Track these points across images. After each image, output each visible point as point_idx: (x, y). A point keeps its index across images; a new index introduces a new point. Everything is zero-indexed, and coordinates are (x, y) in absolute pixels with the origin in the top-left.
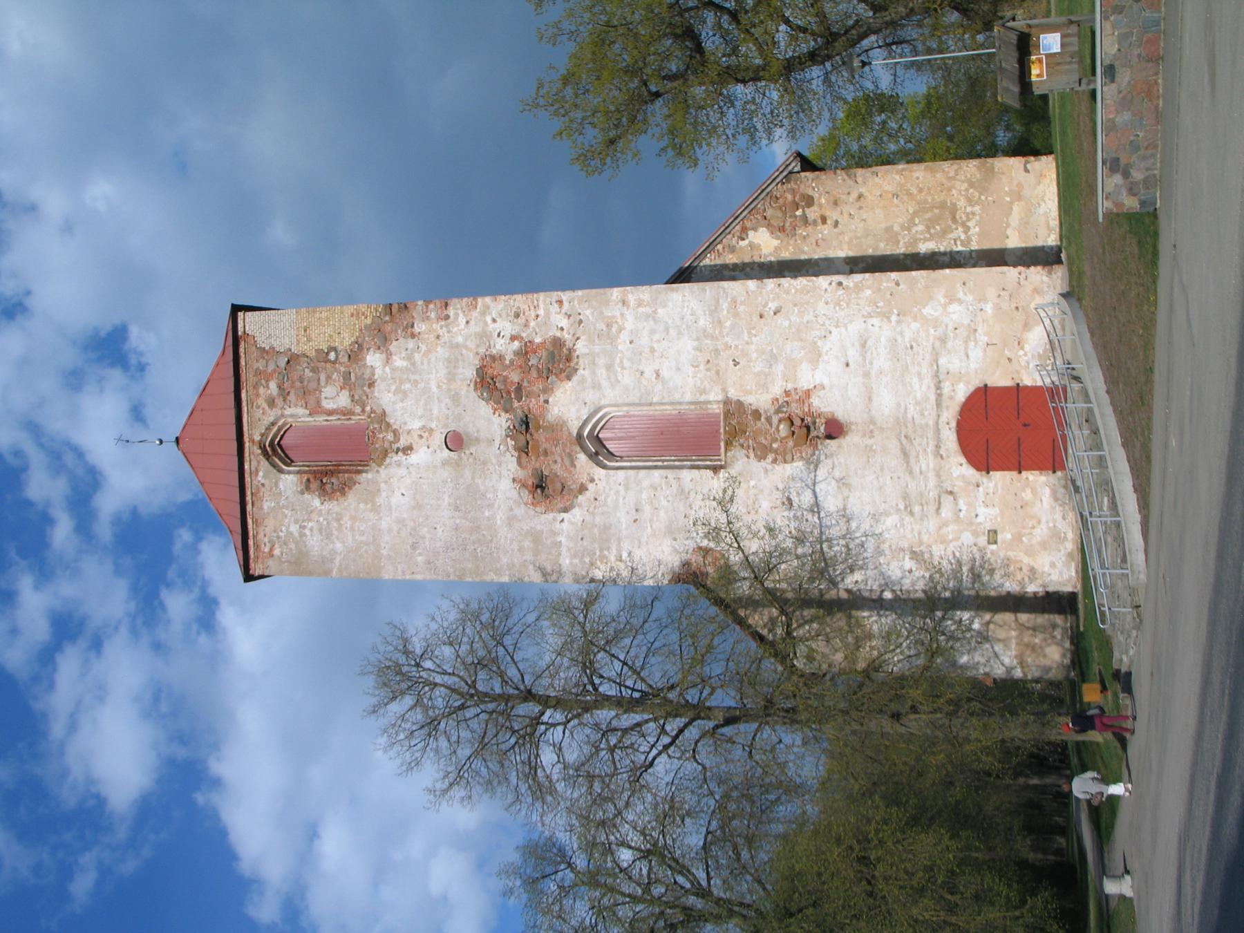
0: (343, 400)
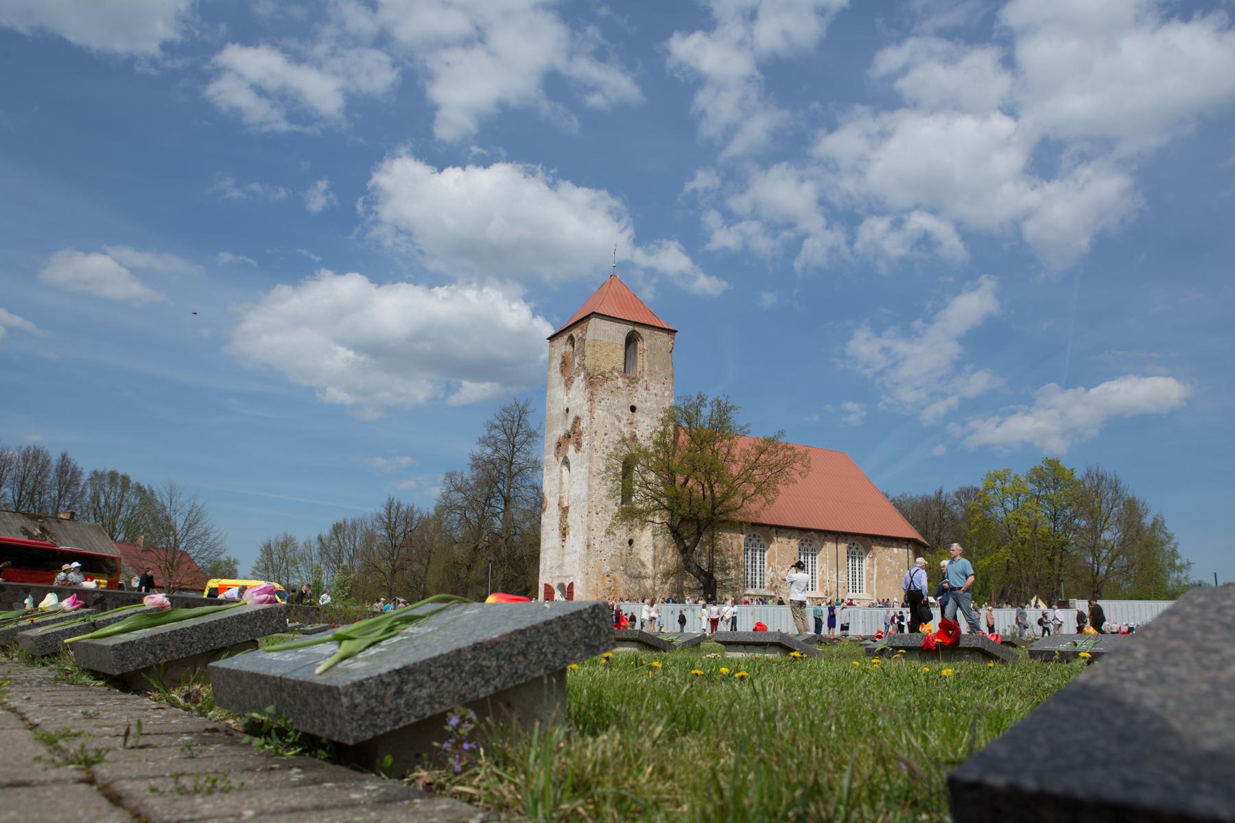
0: (576, 365)
